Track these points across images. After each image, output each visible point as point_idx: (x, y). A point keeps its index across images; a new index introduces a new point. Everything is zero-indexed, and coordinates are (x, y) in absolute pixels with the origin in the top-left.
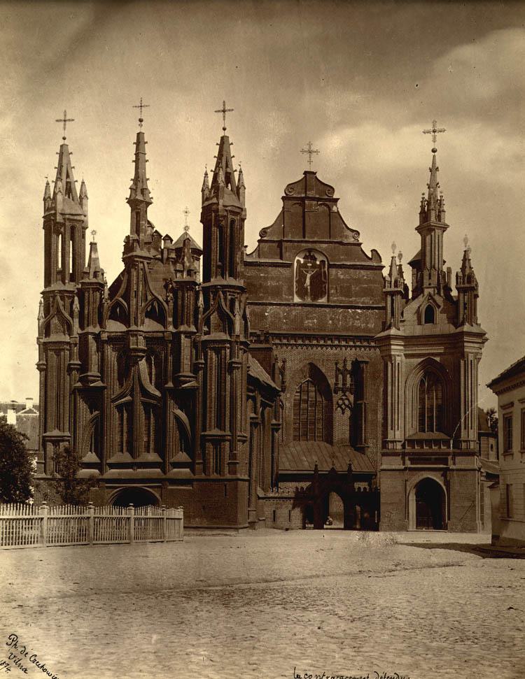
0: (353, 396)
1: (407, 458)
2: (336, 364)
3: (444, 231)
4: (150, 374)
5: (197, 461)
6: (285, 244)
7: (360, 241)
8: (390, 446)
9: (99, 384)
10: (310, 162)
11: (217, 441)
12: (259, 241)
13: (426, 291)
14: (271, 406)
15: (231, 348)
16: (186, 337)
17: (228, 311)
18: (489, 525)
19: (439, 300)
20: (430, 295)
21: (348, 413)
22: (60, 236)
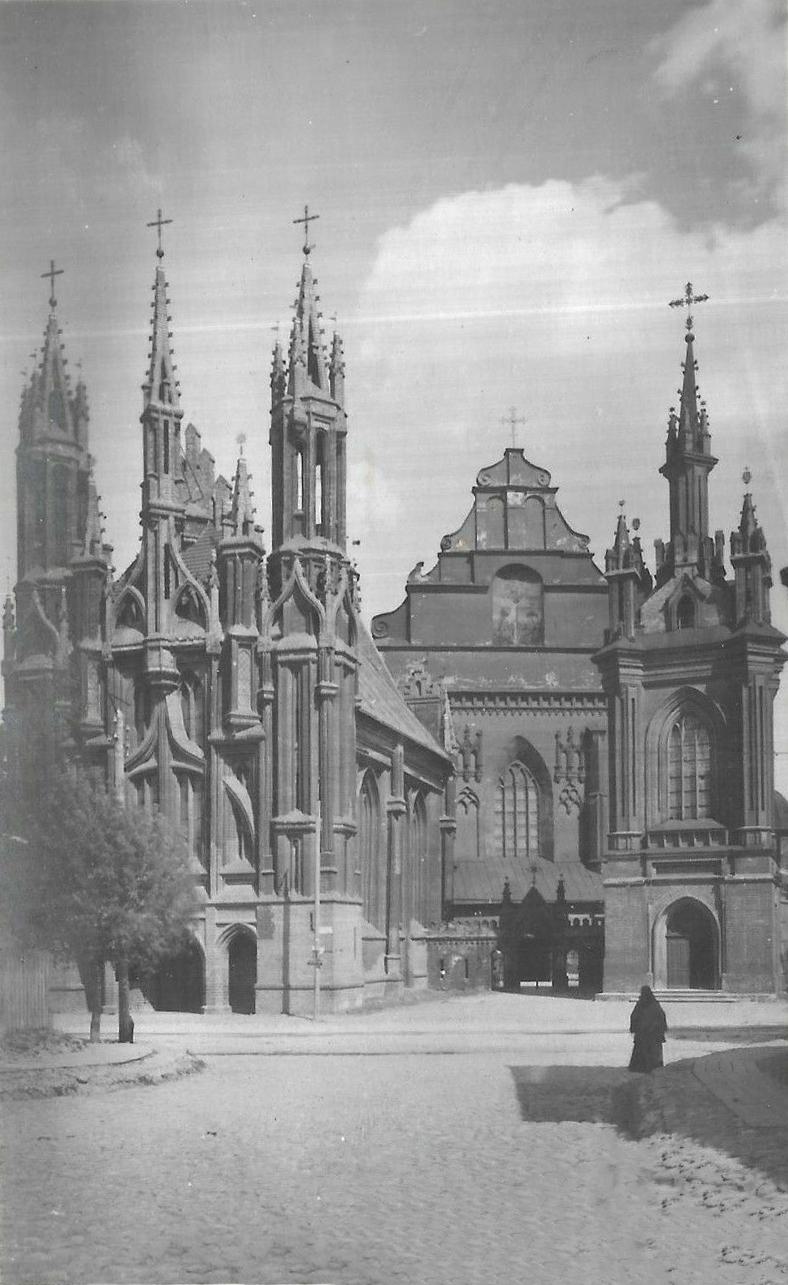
0: (582, 785)
1: (649, 863)
2: (557, 736)
3: (710, 469)
4: (187, 719)
5: (263, 871)
6: (477, 559)
7: (591, 551)
8: (621, 842)
10: (513, 435)
11: (297, 833)
13: (679, 573)
14: (439, 793)
15: (318, 662)
16: (241, 646)
17: (312, 595)
18: (271, 680)
19: (704, 585)
20: (686, 575)
21: (575, 810)
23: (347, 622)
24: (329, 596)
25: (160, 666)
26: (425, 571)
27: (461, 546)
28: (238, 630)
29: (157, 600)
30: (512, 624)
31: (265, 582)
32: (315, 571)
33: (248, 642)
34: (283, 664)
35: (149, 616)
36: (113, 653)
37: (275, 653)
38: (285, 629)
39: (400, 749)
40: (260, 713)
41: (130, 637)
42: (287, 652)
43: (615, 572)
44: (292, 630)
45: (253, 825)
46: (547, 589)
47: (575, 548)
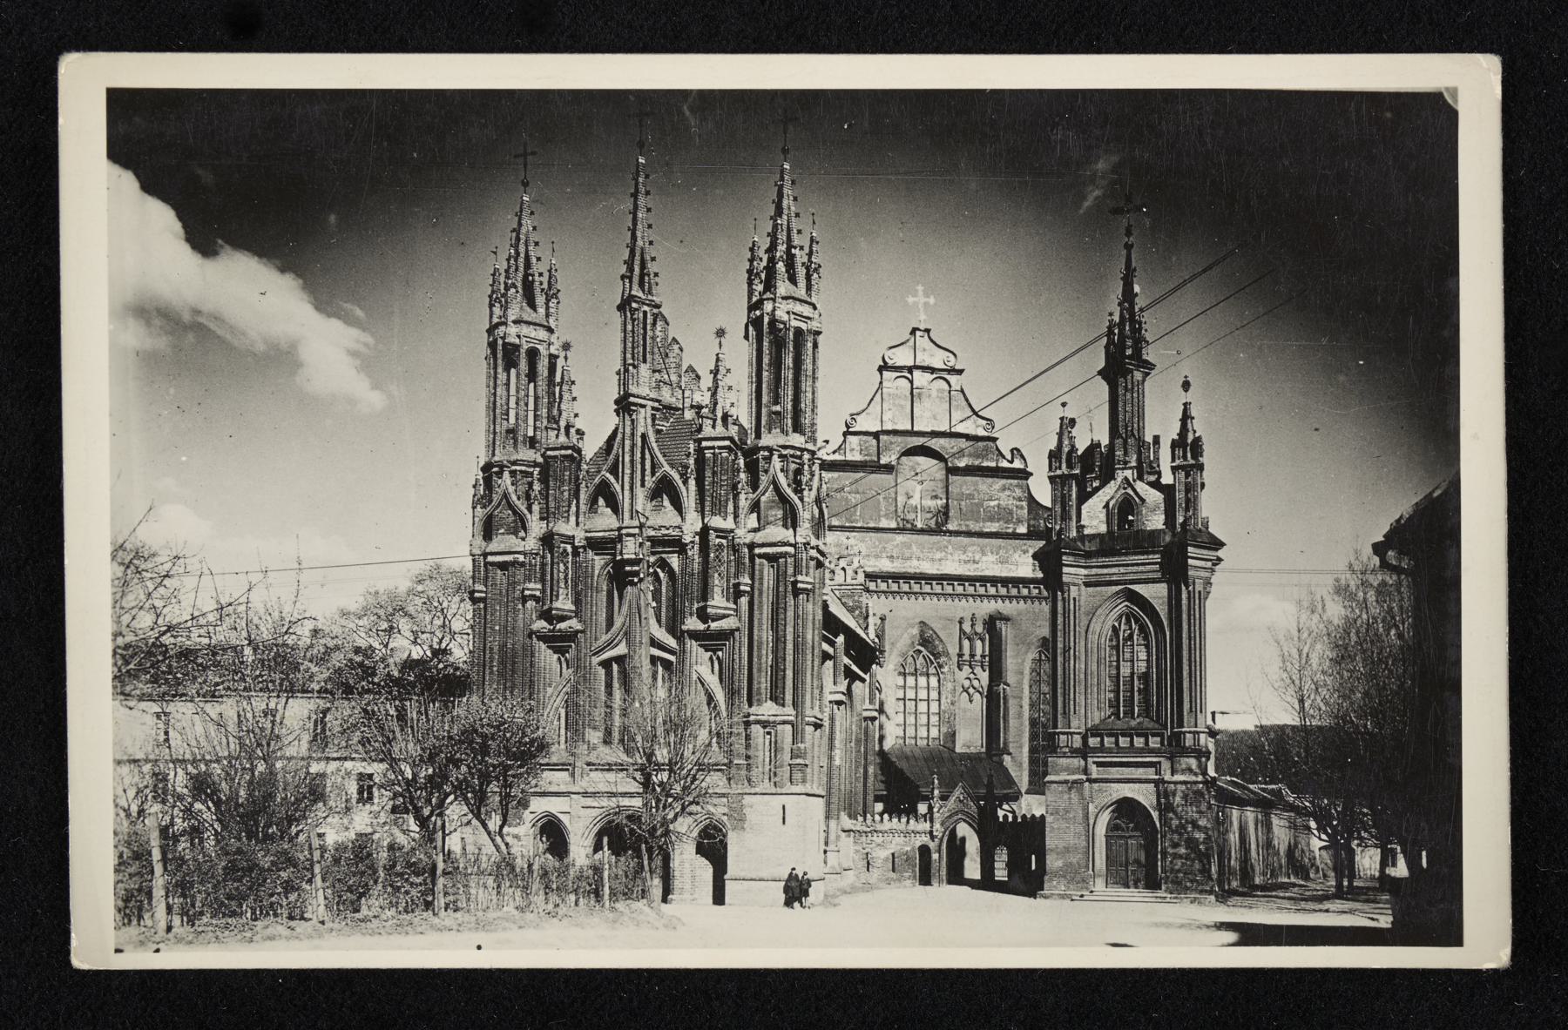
2: (960, 623)
9: (574, 624)
12: (845, 434)
13: (1120, 475)
14: (863, 680)
17: (789, 492)
20: (1126, 479)
27: (863, 424)
28: (716, 522)
32: (793, 466)
33: (722, 533)
34: (760, 556)
36: (587, 539)
37: (751, 546)
38: (762, 522)
39: (840, 639)
41: (604, 521)
42: (763, 545)
43: (1059, 472)
46: (952, 471)
47: (981, 433)
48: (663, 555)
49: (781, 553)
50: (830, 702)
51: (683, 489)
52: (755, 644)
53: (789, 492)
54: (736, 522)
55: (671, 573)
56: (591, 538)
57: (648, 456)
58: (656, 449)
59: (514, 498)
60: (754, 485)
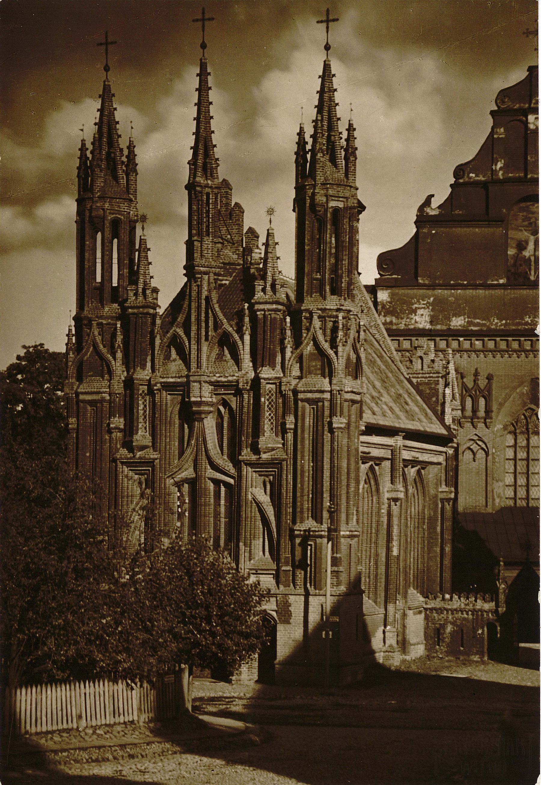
17: (326, 346)
22: (99, 235)
23: (355, 361)
24: (340, 349)
25: (201, 397)
26: (436, 203)
28: (266, 373)
29: (199, 342)
30: (529, 258)
31: (288, 333)
32: (330, 325)
34: (302, 400)
35: (192, 356)
38: (304, 372)
40: (283, 439)
44: (310, 373)
45: (275, 530)
48: (223, 396)
49: (319, 398)
50: (388, 499)
51: (240, 343)
52: (299, 472)
53: (326, 346)
54: (284, 372)
55: (231, 410)
56: (166, 382)
57: (210, 314)
58: (217, 309)
59: (101, 347)
60: (298, 343)
